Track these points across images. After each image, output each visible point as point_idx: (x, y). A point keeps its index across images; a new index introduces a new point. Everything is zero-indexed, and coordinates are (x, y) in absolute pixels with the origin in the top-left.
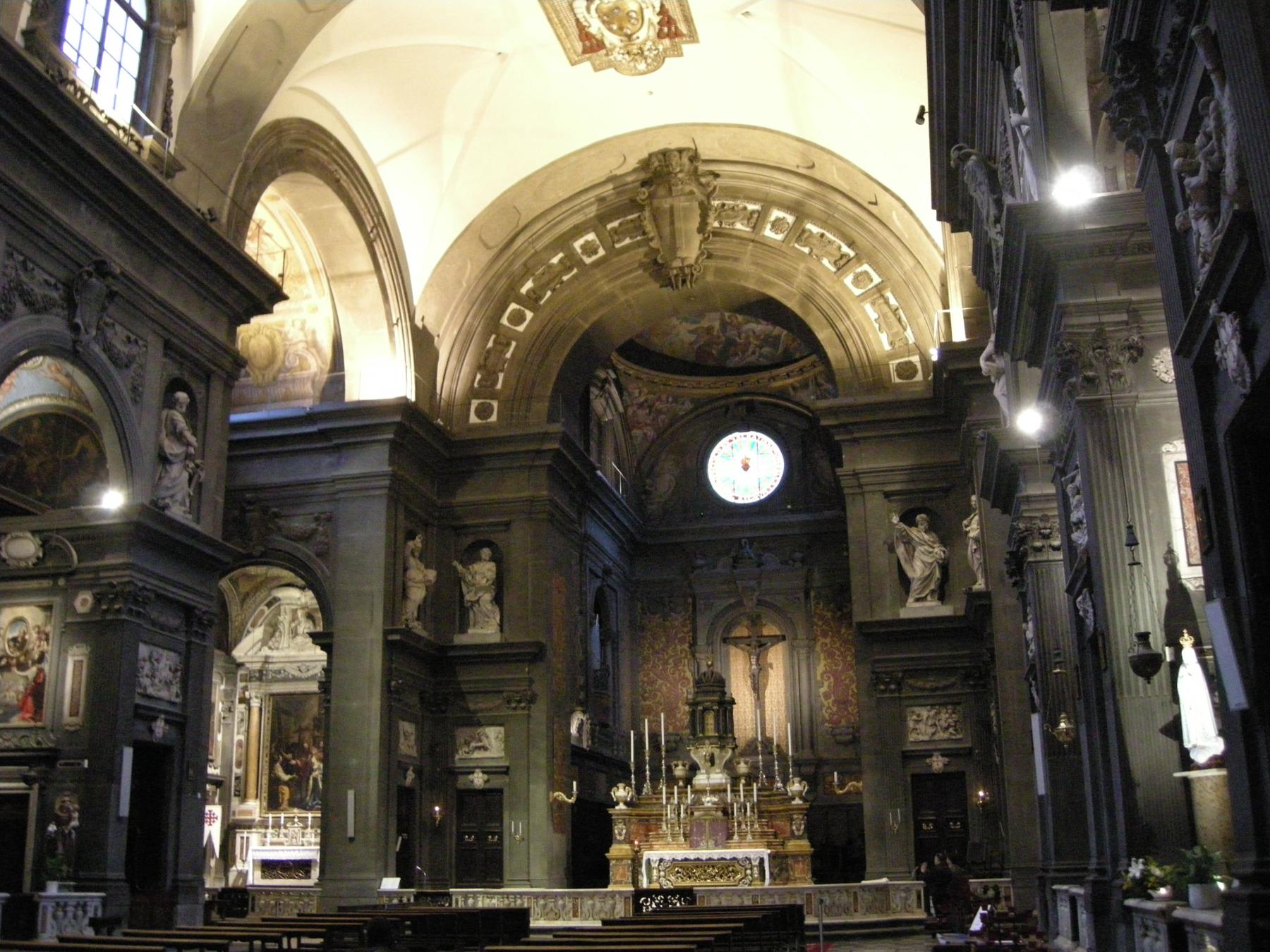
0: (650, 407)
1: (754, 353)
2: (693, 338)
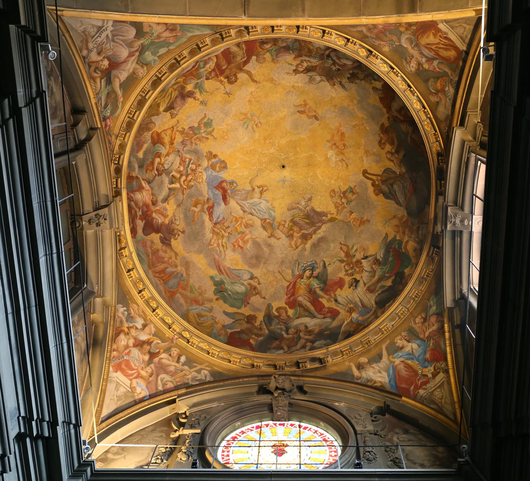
0: (153, 355)
1: (304, 347)
2: (228, 321)
